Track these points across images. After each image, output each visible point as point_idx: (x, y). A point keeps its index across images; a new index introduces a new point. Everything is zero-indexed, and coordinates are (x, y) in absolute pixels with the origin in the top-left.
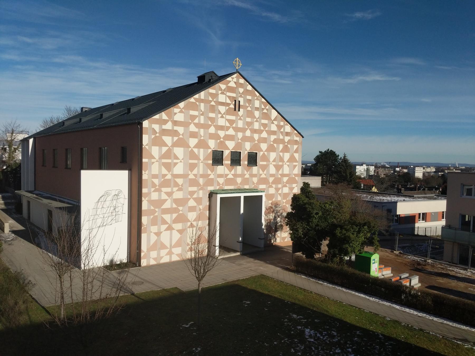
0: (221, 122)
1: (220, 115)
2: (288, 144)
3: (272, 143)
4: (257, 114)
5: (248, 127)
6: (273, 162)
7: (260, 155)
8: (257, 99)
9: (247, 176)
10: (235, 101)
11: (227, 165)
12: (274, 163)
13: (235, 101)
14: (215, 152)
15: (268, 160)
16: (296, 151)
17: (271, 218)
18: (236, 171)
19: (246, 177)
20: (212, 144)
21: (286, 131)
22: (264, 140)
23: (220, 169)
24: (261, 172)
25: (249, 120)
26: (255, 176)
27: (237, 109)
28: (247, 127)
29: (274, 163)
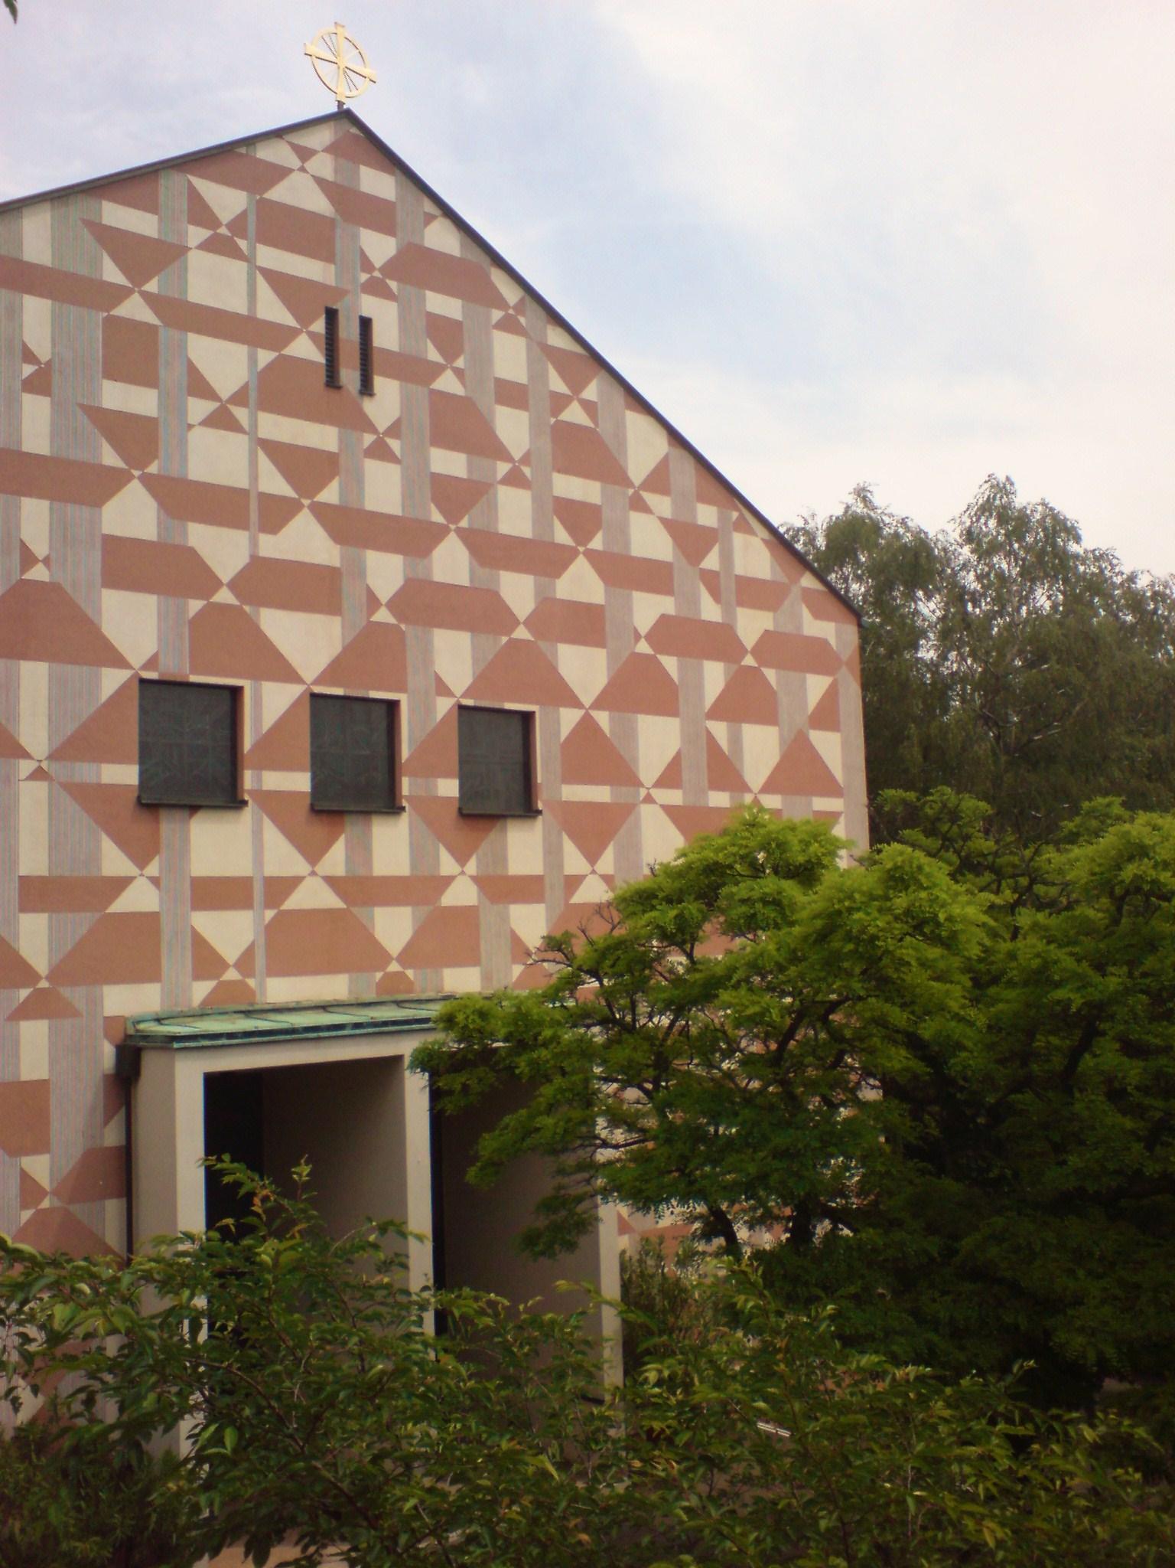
0: (216, 458)
1: (199, 408)
2: (763, 661)
3: (643, 647)
4: (513, 428)
5: (453, 516)
6: (660, 783)
7: (556, 726)
8: (509, 325)
9: (462, 893)
10: (332, 316)
11: (274, 804)
12: (674, 797)
13: (332, 316)
14: (158, 693)
15: (622, 773)
16: (826, 716)
17: (345, 1367)
18: (362, 850)
19: (449, 899)
20: (137, 629)
21: (739, 570)
22: (585, 624)
23: (216, 843)
24: (574, 861)
25: (449, 463)
26: (527, 889)
27: (350, 376)
28: (437, 517)
29: (674, 797)
